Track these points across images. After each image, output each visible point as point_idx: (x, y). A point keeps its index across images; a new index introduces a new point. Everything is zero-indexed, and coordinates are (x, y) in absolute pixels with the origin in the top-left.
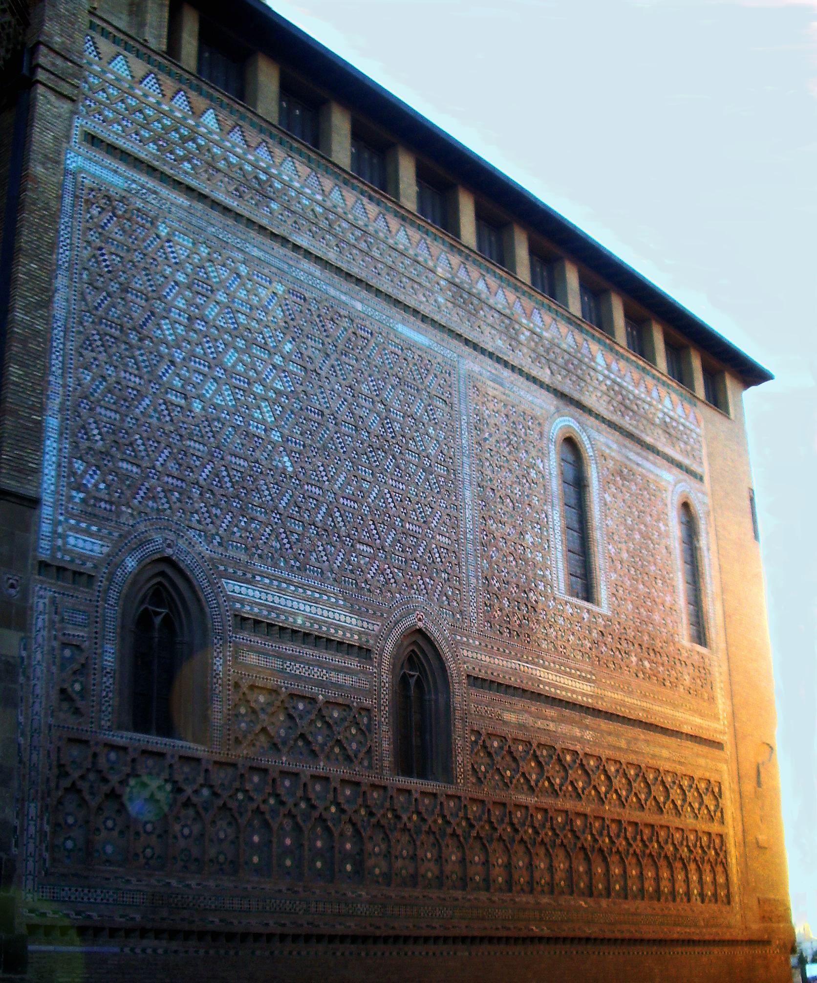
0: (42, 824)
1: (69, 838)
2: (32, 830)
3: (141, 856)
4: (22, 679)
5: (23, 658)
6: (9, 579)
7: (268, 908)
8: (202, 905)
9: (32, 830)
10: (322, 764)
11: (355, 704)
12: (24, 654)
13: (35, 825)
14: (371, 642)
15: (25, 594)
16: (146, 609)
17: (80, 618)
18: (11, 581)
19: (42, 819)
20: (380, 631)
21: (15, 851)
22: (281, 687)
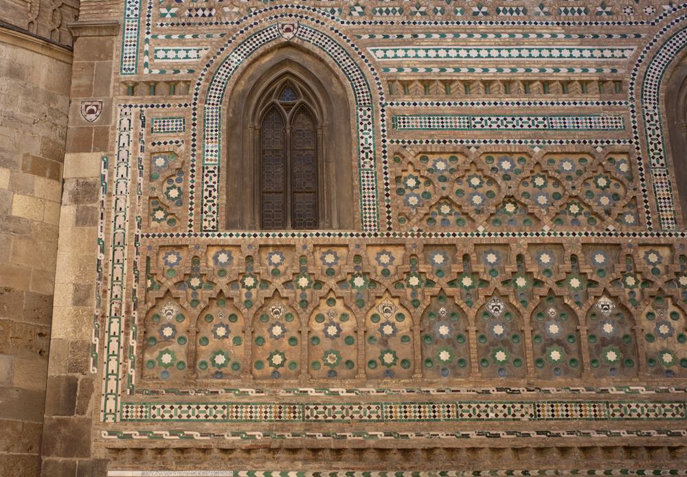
0: (127, 340)
1: (167, 351)
2: (114, 346)
3: (267, 364)
4: (102, 197)
5: (103, 177)
6: (87, 106)
7: (466, 415)
8: (356, 416)
9: (114, 346)
10: (546, 229)
11: (599, 149)
12: (105, 172)
13: (119, 341)
14: (620, 71)
15: (107, 115)
16: (273, 103)
17: (172, 125)
18: (88, 108)
19: (127, 334)
20: (636, 56)
21: (93, 370)
22: (469, 147)
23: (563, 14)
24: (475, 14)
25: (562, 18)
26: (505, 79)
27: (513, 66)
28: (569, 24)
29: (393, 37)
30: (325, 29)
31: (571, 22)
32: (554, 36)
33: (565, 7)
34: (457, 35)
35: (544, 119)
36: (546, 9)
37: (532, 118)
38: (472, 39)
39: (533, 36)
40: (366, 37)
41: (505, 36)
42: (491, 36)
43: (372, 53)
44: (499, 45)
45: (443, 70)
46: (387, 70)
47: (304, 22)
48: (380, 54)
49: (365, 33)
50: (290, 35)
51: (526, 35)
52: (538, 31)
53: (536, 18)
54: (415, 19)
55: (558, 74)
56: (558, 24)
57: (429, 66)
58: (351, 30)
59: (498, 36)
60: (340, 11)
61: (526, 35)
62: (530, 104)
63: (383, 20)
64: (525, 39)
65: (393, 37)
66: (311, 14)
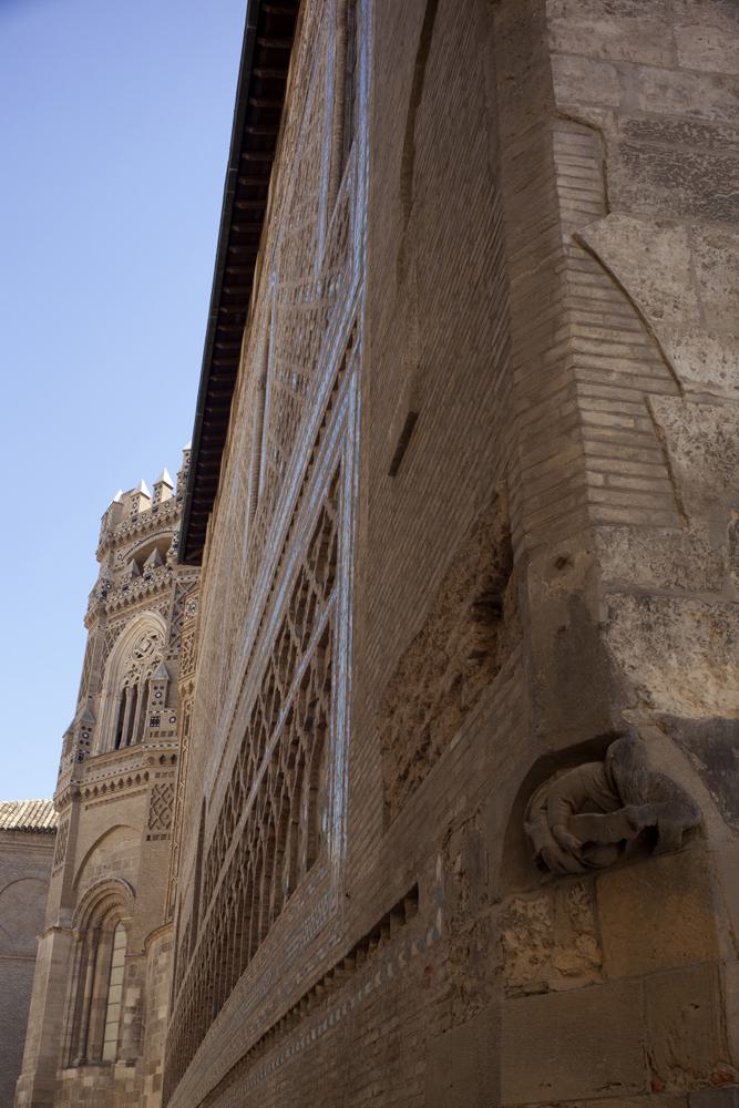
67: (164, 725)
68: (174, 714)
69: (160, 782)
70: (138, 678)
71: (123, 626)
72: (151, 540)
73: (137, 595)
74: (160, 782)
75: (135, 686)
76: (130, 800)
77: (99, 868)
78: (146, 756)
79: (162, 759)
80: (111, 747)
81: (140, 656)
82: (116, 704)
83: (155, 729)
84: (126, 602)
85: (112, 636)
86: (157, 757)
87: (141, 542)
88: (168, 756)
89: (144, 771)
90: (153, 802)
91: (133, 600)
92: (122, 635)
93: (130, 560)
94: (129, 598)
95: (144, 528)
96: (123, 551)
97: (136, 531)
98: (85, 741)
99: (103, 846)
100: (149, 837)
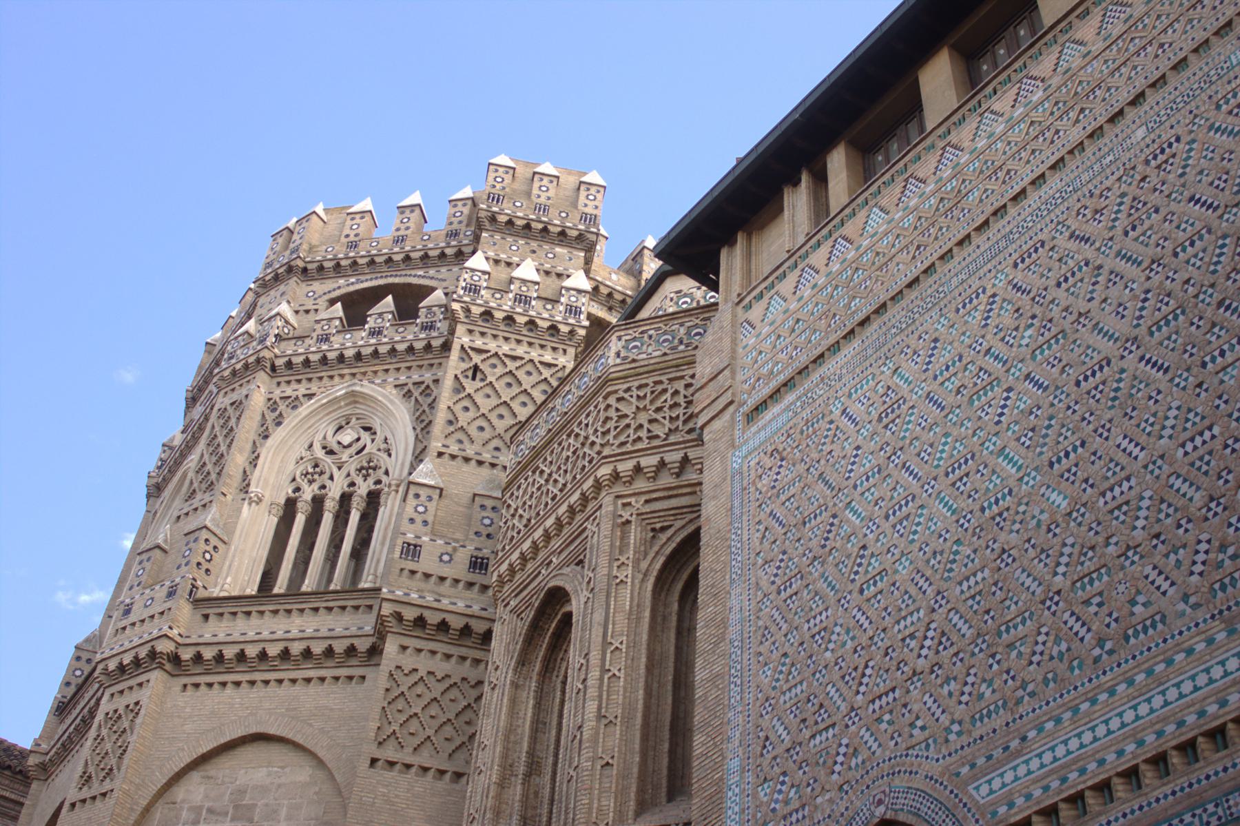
23: (1220, 594)
24: (1097, 660)
25: (1218, 605)
26: (1149, 755)
27: (1157, 727)
28: (1229, 608)
29: (997, 753)
30: (919, 782)
31: (1231, 604)
32: (1210, 641)
33: (1220, 580)
34: (1075, 710)
35: (1217, 806)
36: (1192, 600)
37: (1198, 812)
38: (1097, 708)
39: (1179, 657)
40: (965, 770)
41: (1140, 678)
42: (1121, 688)
43: (974, 793)
44: (1134, 698)
45: (1064, 780)
46: (994, 813)
47: (897, 782)
48: (984, 789)
49: (963, 764)
50: (882, 809)
51: (1169, 662)
52: (1186, 645)
53: (1179, 623)
54: (1021, 710)
55: (1227, 709)
56: (1213, 617)
57: (1045, 782)
58: (947, 768)
59: (1130, 682)
60: (935, 741)
61: (1169, 662)
62: (1191, 785)
63: (983, 731)
64: (1170, 669)
65: (997, 753)
66: (903, 765)
67: (427, 562)
68: (449, 549)
69: (408, 661)
70: (323, 487)
71: (310, 396)
72: (381, 282)
73: (349, 353)
74: (408, 661)
75: (318, 502)
76: (298, 689)
77: (197, 810)
78: (387, 609)
79: (420, 622)
80: (252, 590)
81: (331, 452)
82: (268, 524)
83: (410, 565)
84: (324, 360)
85: (282, 407)
86: (410, 614)
87: (358, 281)
88: (433, 618)
89: (347, 642)
90: (394, 697)
91: (341, 358)
92: (306, 408)
93: (332, 302)
94: (332, 356)
95: (372, 262)
96: (318, 287)
97: (355, 263)
98: (205, 566)
99: (212, 769)
100: (374, 761)
